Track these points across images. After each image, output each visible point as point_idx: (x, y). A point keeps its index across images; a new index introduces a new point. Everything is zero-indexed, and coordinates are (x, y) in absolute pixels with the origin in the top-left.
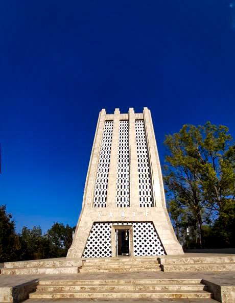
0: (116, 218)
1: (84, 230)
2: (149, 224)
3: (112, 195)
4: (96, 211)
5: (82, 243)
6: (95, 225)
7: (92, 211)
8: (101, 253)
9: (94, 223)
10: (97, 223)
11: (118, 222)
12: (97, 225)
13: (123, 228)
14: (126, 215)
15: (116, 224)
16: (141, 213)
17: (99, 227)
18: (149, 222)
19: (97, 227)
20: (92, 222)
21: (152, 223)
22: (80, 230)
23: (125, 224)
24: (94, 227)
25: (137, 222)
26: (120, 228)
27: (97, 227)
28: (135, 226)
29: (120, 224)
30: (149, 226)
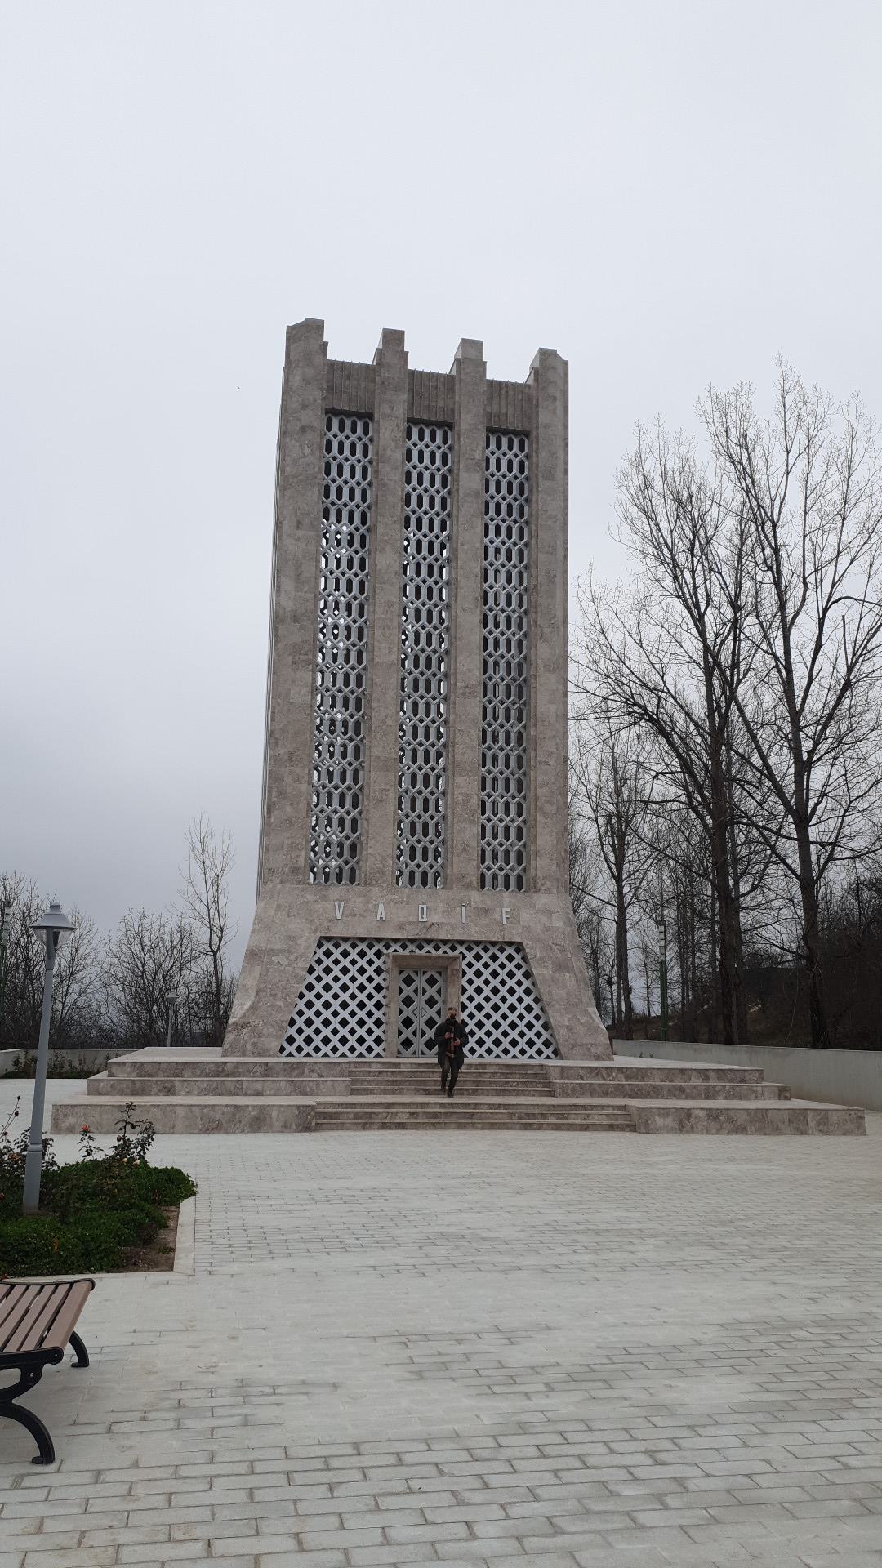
0: (401, 927)
2: (510, 950)
3: (381, 840)
4: (324, 899)
5: (280, 1003)
6: (320, 945)
7: (310, 897)
9: (320, 945)
10: (328, 939)
12: (328, 946)
14: (436, 919)
16: (486, 911)
18: (510, 944)
19: (328, 954)
20: (315, 938)
21: (519, 948)
27: (328, 954)
29: (411, 947)
30: (510, 958)
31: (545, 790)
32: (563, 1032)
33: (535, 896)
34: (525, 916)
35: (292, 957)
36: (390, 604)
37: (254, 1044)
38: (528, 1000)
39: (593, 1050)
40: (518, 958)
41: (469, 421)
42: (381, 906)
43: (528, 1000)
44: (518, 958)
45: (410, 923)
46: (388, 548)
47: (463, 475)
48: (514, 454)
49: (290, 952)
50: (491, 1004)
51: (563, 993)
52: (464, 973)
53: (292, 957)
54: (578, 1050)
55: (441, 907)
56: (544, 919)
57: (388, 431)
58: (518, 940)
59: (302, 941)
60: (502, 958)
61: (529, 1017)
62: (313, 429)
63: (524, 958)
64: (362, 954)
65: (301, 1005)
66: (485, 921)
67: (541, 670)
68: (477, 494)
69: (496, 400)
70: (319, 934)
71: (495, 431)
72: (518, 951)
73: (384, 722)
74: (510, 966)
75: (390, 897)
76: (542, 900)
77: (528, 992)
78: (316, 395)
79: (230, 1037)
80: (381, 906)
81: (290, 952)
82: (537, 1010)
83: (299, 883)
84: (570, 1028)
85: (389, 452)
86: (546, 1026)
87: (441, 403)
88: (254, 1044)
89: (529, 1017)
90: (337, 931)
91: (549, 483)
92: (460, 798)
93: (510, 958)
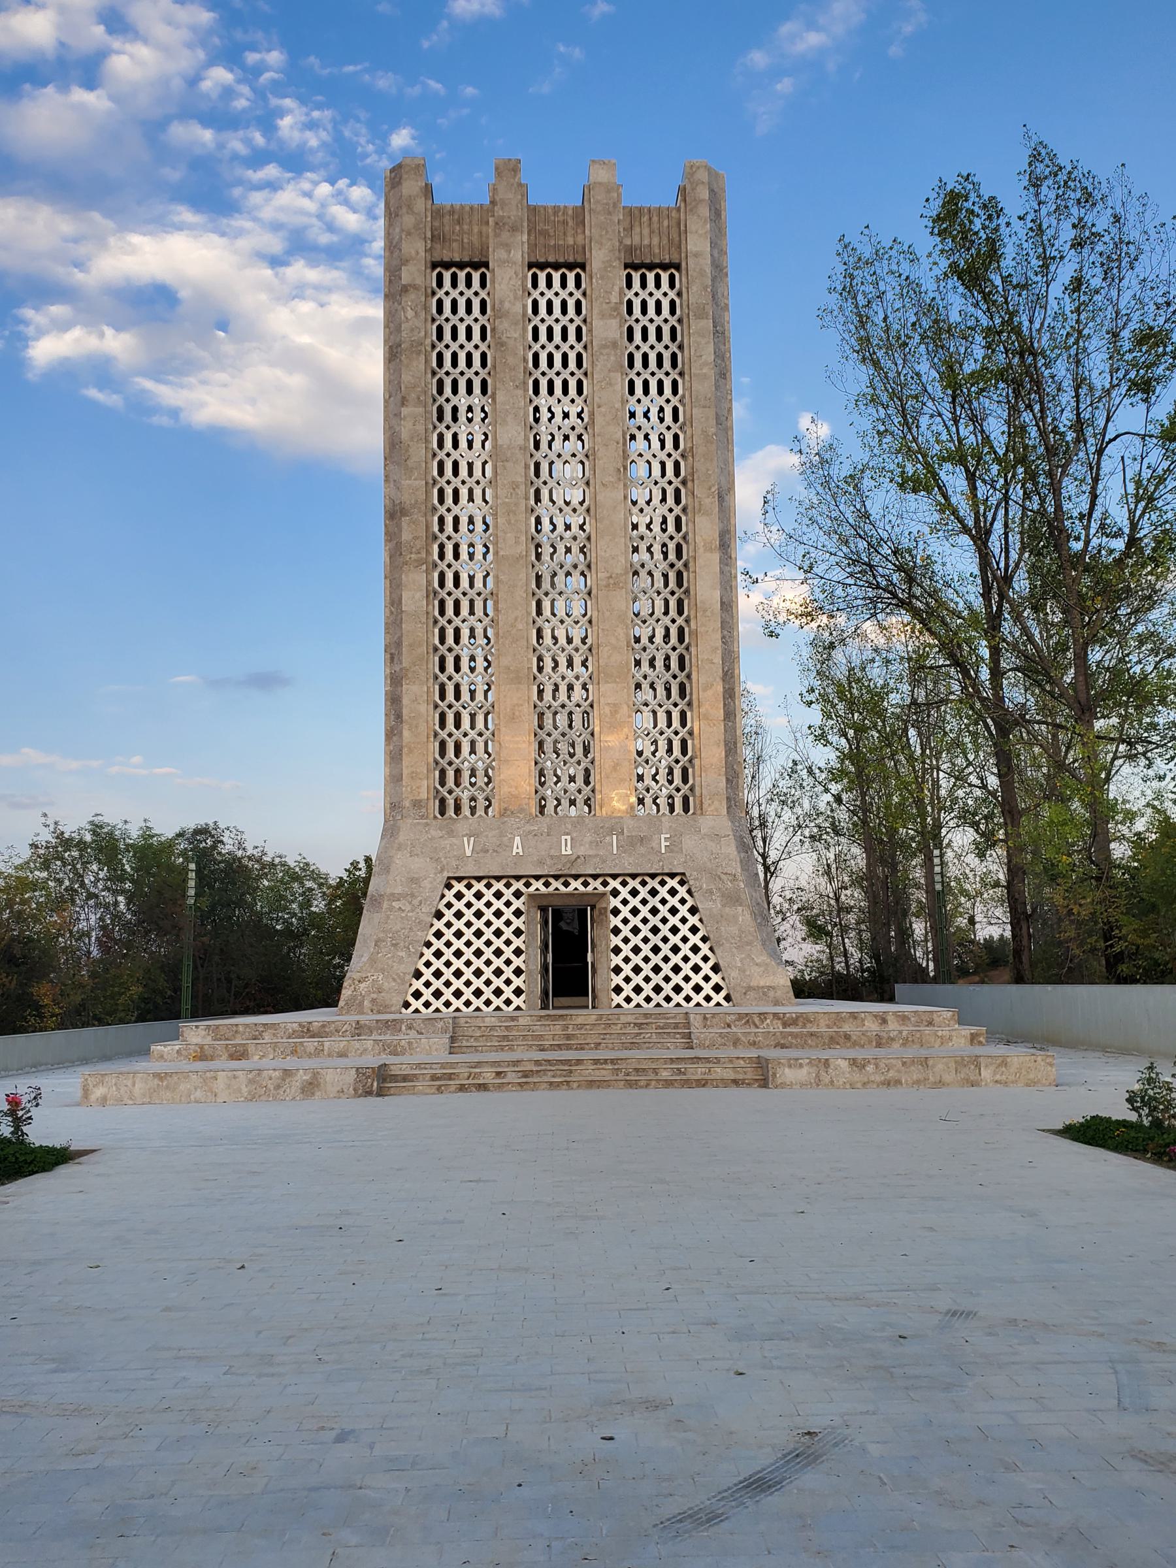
0: (541, 863)
1: (408, 908)
2: (672, 883)
4: (451, 833)
5: (403, 954)
6: (449, 886)
7: (434, 833)
8: (437, 994)
12: (459, 887)
14: (582, 851)
15: (538, 885)
17: (469, 895)
19: (459, 896)
22: (391, 908)
23: (576, 884)
27: (459, 896)
28: (615, 893)
29: (555, 884)
32: (734, 974)
33: (701, 819)
36: (515, 486)
37: (373, 1001)
38: (695, 939)
39: (771, 994)
40: (682, 892)
41: (602, 258)
42: (517, 839)
43: (695, 939)
44: (682, 892)
45: (552, 857)
46: (509, 419)
47: (596, 323)
48: (665, 294)
49: (413, 895)
50: (650, 945)
51: (734, 930)
54: (751, 994)
55: (589, 837)
56: (712, 845)
57: (507, 277)
59: (426, 884)
60: (663, 892)
61: (696, 959)
62: (416, 287)
63: (689, 892)
64: (498, 895)
65: (428, 954)
66: (642, 850)
67: (701, 551)
68: (614, 345)
69: (637, 230)
70: (446, 874)
71: (636, 265)
72: (682, 883)
73: (513, 626)
74: (673, 901)
75: (528, 828)
77: (694, 930)
78: (416, 249)
79: (346, 993)
80: (517, 839)
81: (413, 895)
82: (705, 949)
83: (422, 817)
84: (742, 970)
85: (507, 305)
86: (716, 969)
87: (570, 241)
88: (373, 1001)
89: (696, 959)
90: (470, 870)
91: (703, 323)
92: (607, 710)
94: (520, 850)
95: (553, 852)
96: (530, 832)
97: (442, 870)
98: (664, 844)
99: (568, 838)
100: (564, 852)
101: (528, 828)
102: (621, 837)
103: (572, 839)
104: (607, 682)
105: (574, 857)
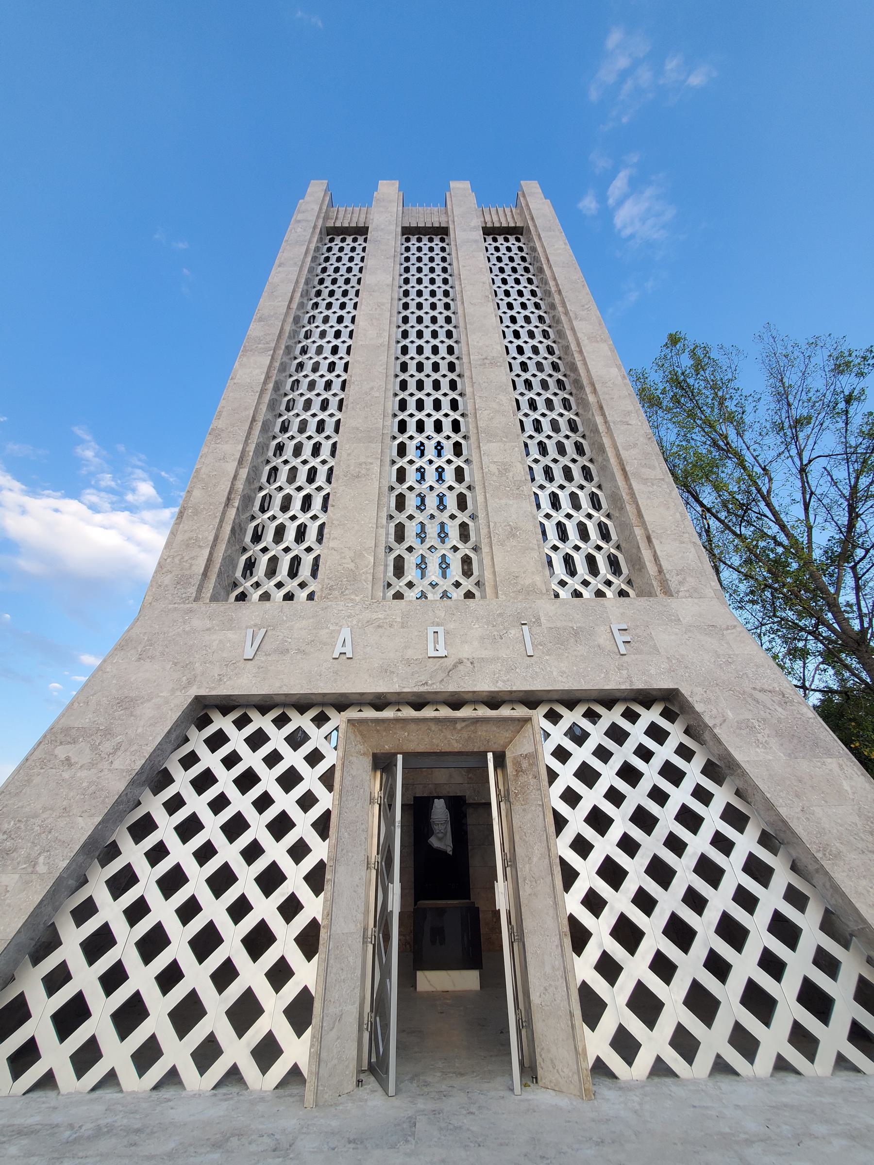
0: (386, 671)
2: (650, 716)
6: (203, 722)
10: (225, 706)
11: (379, 702)
12: (223, 723)
13: (451, 742)
14: (465, 652)
18: (647, 699)
19: (217, 741)
20: (182, 701)
24: (197, 741)
25: (556, 703)
26: (418, 742)
27: (217, 741)
31: (633, 452)
34: (665, 638)
35: (107, 746)
42: (346, 633)
43: (746, 843)
45: (408, 662)
49: (108, 733)
52: (553, 776)
53: (107, 746)
58: (665, 683)
59: (147, 711)
75: (367, 615)
76: (685, 608)
80: (346, 633)
92: (493, 468)
93: (657, 733)
94: (348, 650)
95: (410, 653)
96: (369, 622)
97: (190, 683)
98: (620, 638)
99: (440, 630)
100: (432, 653)
101: (367, 615)
102: (536, 630)
103: (447, 633)
104: (489, 441)
105: (449, 662)
